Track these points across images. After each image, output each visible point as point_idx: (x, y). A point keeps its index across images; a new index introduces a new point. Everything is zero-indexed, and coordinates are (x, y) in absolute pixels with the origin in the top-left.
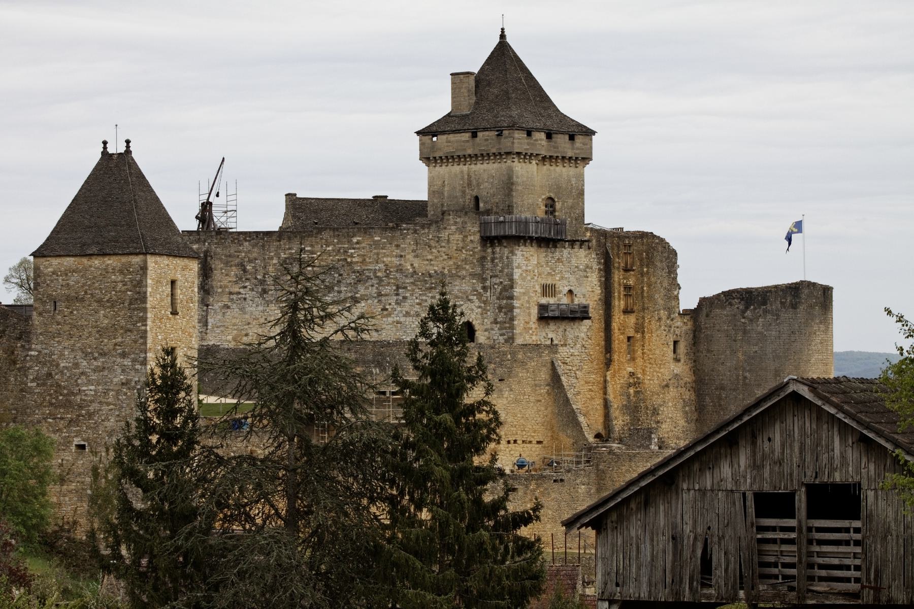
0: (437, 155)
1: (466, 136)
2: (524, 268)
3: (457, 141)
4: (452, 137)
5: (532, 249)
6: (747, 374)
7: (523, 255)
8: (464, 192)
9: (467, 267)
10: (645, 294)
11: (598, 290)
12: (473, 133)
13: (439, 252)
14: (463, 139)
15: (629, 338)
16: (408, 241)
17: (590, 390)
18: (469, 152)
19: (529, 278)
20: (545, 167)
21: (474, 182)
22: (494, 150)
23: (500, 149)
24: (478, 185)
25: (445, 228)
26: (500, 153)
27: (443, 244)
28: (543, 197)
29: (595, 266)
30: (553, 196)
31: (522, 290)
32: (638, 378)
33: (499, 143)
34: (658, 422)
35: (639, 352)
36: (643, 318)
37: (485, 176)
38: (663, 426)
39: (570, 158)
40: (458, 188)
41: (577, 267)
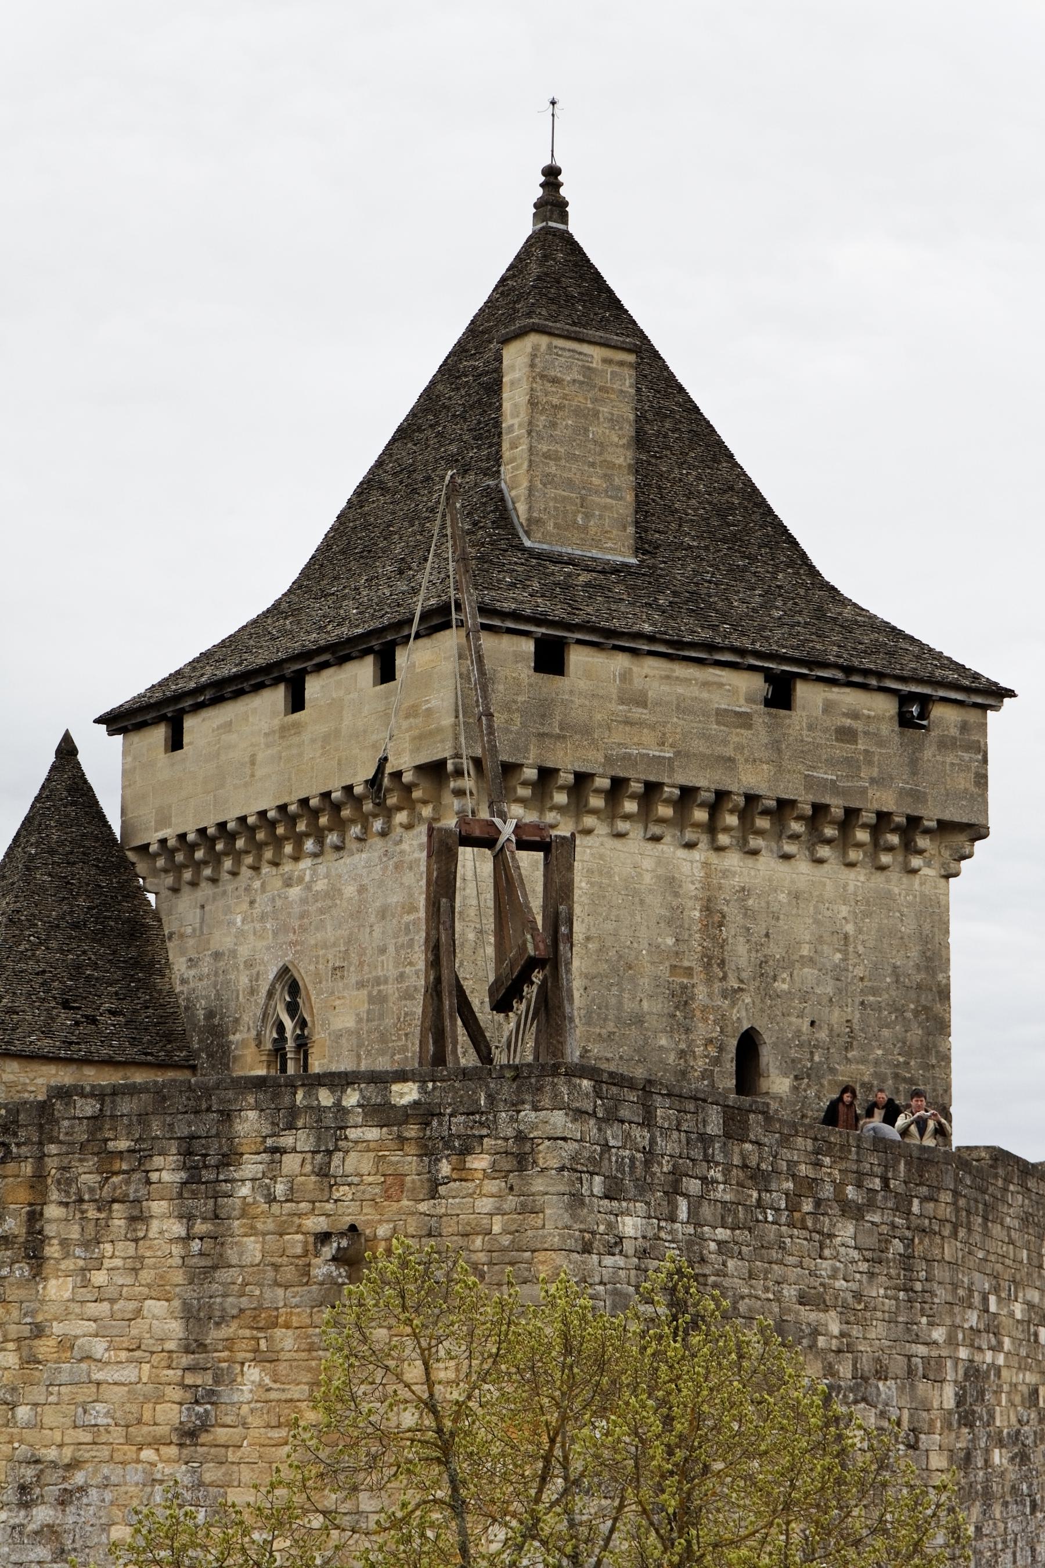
0: (567, 760)
1: (744, 687)
3: (682, 708)
4: (651, 674)
8: (682, 998)
12: (770, 676)
14: (720, 701)
18: (752, 779)
21: (741, 954)
22: (886, 800)
23: (917, 796)
24: (764, 972)
26: (914, 822)
33: (914, 764)
37: (803, 931)
40: (651, 972)
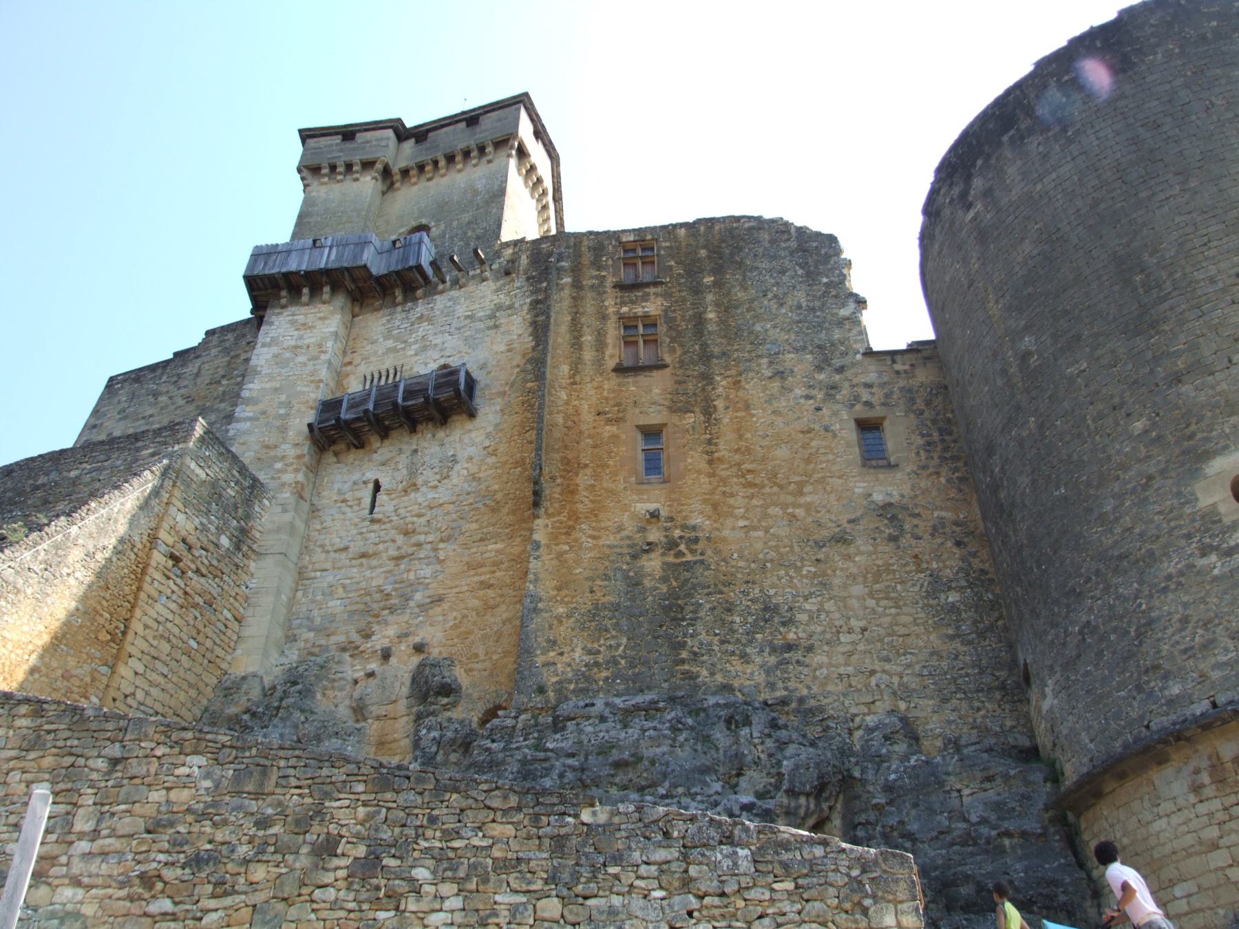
2: (293, 343)
5: (324, 308)
6: (1028, 342)
7: (292, 322)
9: (223, 405)
10: (712, 327)
11: (529, 342)
13: (171, 398)
15: (651, 433)
16: (116, 400)
17: (486, 585)
19: (301, 359)
20: (416, 188)
25: (197, 357)
27: (186, 383)
28: (402, 230)
29: (524, 302)
30: (424, 221)
31: (268, 386)
32: (694, 528)
34: (790, 647)
35: (688, 459)
36: (707, 378)
38: (818, 658)
39: (467, 154)
41: (467, 317)
